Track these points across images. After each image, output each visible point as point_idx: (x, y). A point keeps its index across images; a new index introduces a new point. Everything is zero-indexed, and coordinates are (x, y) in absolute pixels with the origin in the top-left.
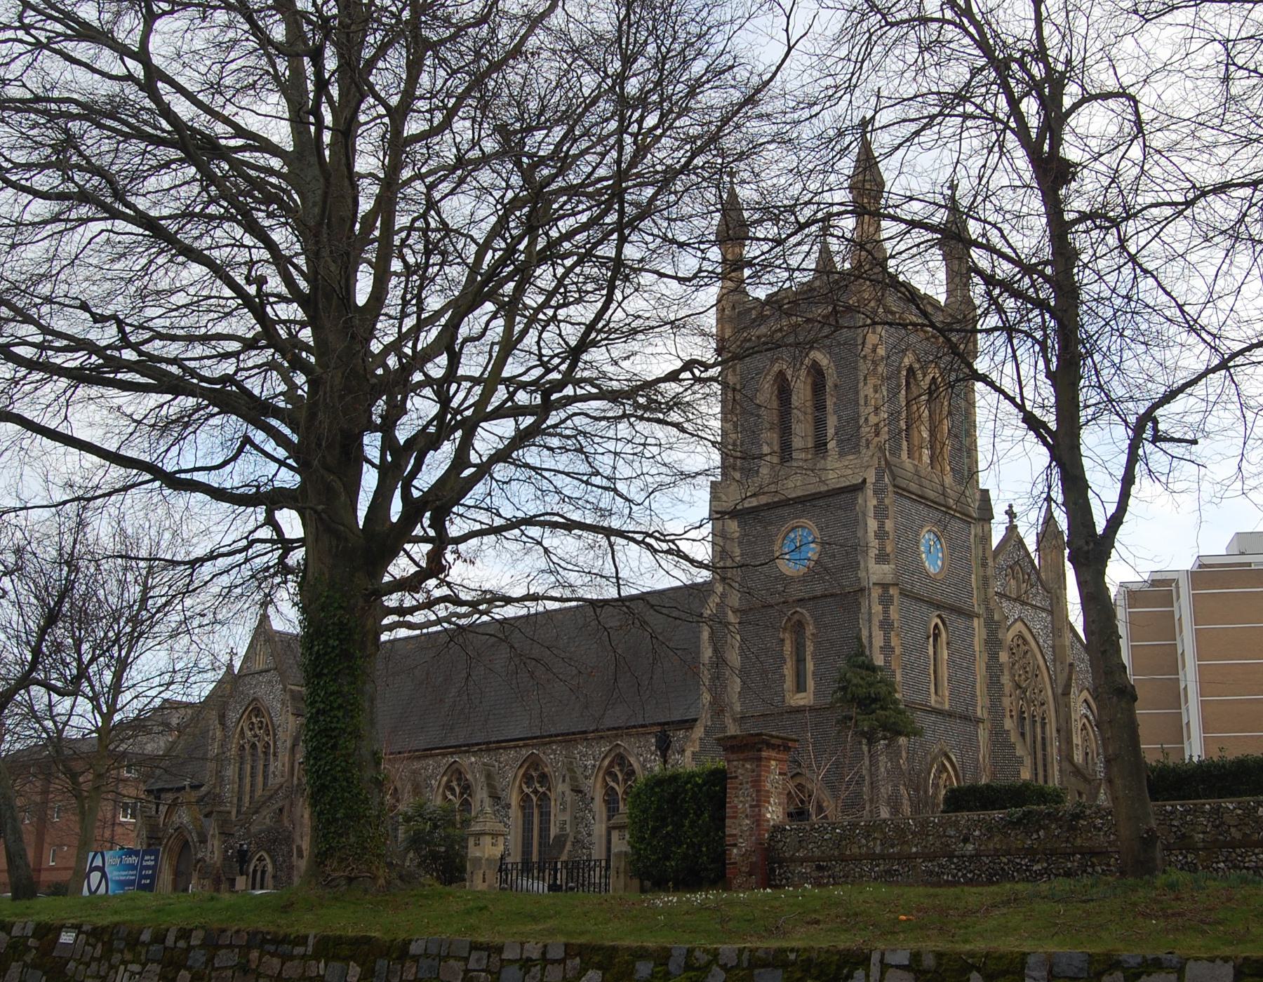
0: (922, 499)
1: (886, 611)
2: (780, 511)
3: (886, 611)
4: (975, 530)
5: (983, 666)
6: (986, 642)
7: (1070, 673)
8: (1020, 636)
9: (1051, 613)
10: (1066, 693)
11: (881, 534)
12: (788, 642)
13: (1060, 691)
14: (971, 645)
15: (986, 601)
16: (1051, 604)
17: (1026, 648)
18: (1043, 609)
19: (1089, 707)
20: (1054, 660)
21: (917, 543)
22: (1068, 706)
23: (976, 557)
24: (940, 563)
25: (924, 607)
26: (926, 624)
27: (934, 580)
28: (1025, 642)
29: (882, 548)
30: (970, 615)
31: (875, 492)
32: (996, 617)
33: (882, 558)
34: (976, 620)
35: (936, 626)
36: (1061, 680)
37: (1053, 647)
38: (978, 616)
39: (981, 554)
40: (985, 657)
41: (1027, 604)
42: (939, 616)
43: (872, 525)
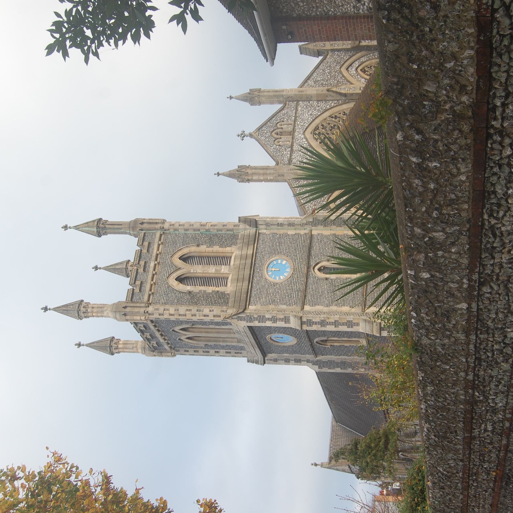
0: (250, 280)
1: (316, 323)
2: (262, 342)
3: (316, 323)
4: (263, 230)
5: (339, 228)
6: (325, 226)
7: (332, 91)
8: (313, 133)
9: (298, 101)
10: (345, 95)
11: (274, 319)
12: (332, 344)
13: (343, 98)
14: (327, 237)
15: (302, 225)
16: (293, 101)
17: (321, 127)
18: (297, 110)
19: (351, 65)
20: (326, 101)
21: (275, 284)
22: (352, 94)
23: (278, 229)
24: (284, 262)
25: (310, 280)
26: (319, 279)
27: (294, 269)
28: (317, 128)
29: (281, 320)
30: (312, 236)
31: (251, 321)
32: (311, 220)
33: (286, 320)
34: (314, 232)
35: (319, 270)
36: (339, 97)
37: (318, 101)
38: (311, 231)
39: (276, 227)
40: (333, 227)
41: (294, 126)
42: (314, 268)
43: (269, 324)
